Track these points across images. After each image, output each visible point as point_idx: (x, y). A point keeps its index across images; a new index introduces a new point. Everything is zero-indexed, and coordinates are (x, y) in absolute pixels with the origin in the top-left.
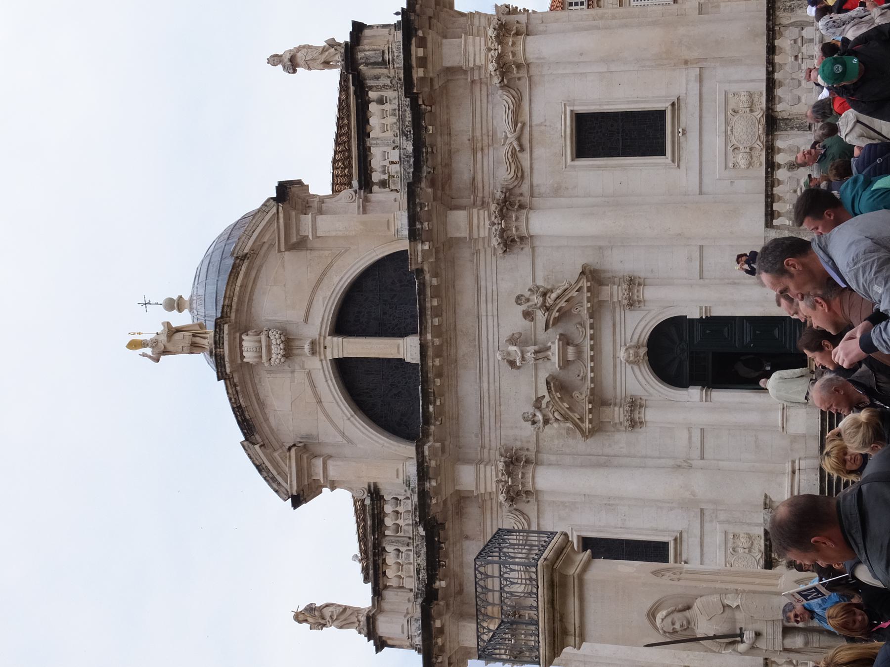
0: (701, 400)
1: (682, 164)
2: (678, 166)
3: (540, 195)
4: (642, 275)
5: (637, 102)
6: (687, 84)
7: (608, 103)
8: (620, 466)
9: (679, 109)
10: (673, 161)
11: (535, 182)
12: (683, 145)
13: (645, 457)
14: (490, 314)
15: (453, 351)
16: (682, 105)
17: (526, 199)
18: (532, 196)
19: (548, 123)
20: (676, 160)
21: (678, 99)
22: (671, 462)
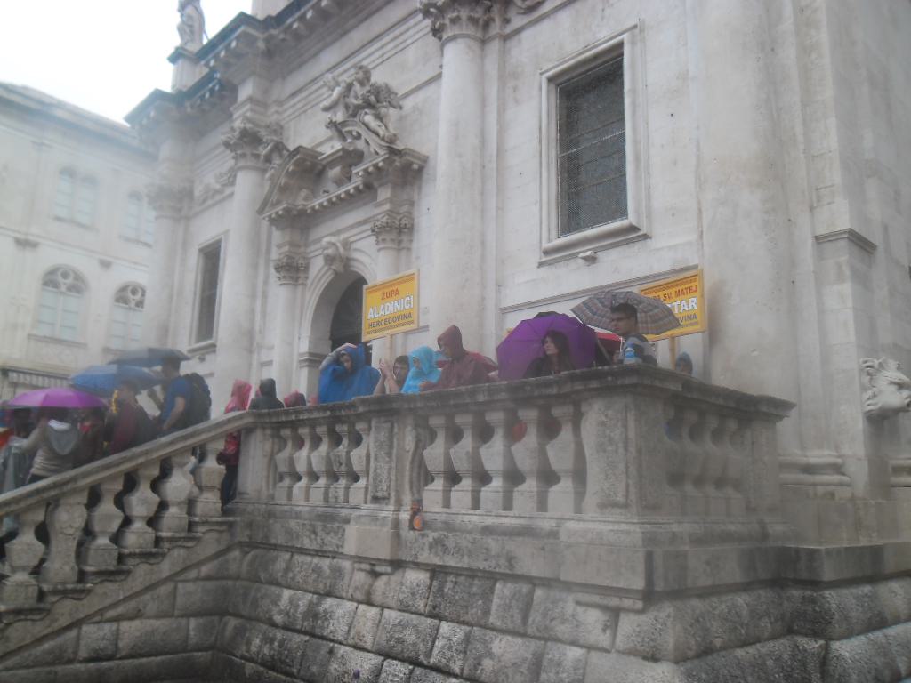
0: (301, 355)
1: (545, 269)
2: (541, 265)
3: (504, 53)
4: (414, 245)
5: (637, 159)
6: (670, 248)
7: (634, 104)
8: (255, 266)
9: (628, 242)
10: (546, 252)
11: (525, 35)
12: (573, 264)
13: (265, 296)
14: (384, 50)
15: (352, 22)
16: (638, 245)
17: (495, 28)
18: (506, 38)
19: (608, 11)
20: (552, 256)
21: (646, 237)
22: (257, 328)
